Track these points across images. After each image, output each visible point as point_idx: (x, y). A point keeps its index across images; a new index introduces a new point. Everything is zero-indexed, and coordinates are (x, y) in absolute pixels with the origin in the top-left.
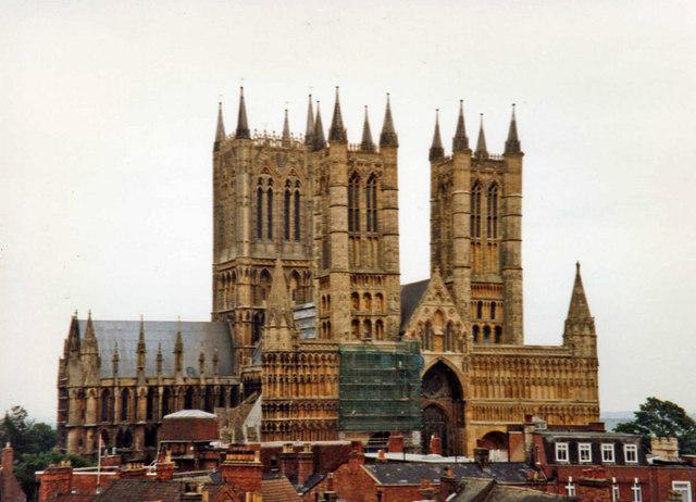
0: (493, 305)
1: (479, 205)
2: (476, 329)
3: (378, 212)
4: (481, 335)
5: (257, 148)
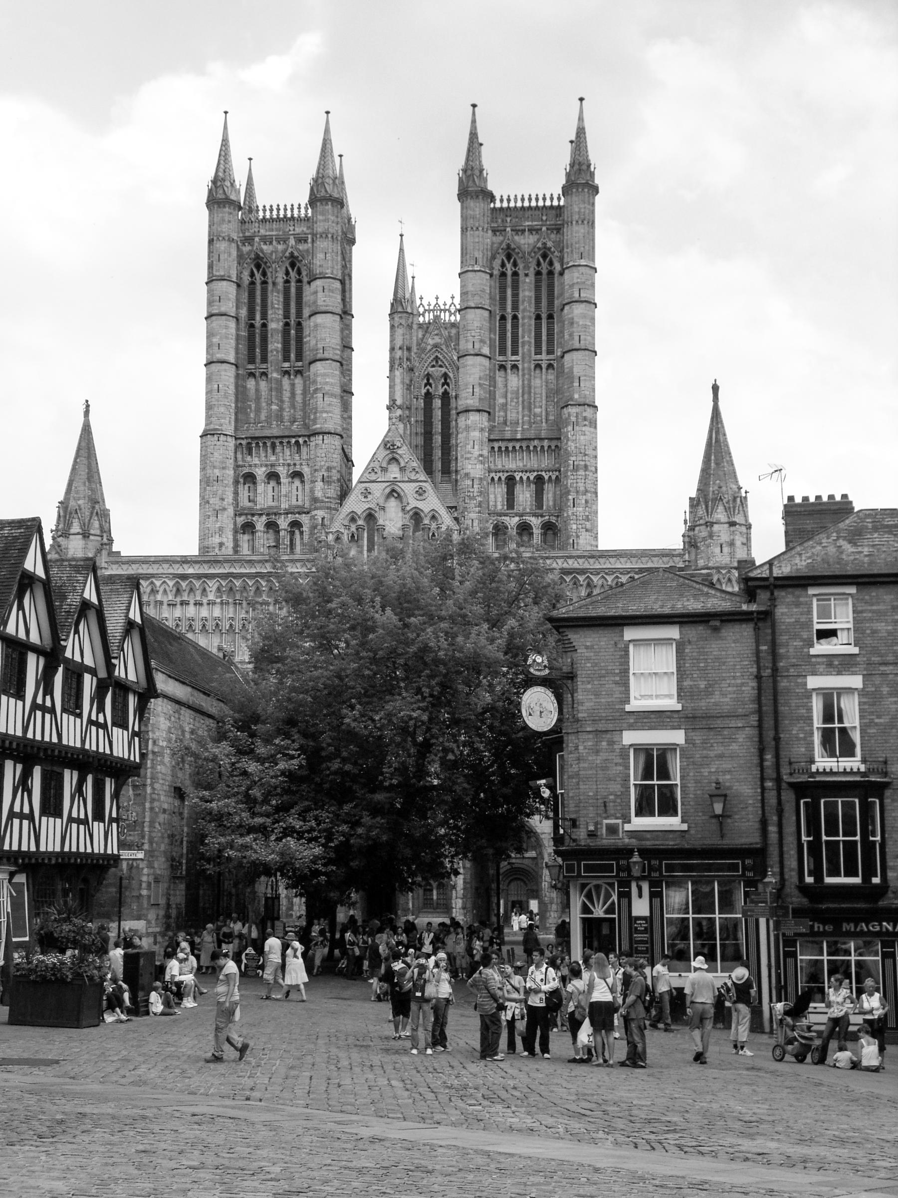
0: (539, 480)
1: (515, 295)
2: (499, 530)
3: (304, 324)
5: (420, 326)
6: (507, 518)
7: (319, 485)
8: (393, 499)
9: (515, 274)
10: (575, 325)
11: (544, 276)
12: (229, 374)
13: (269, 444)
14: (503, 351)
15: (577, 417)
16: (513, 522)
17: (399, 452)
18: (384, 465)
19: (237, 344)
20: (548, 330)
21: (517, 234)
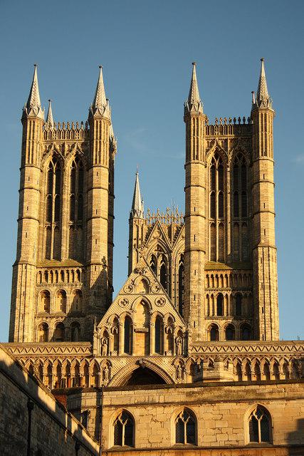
2: (214, 330)
4: (222, 335)
10: (261, 197)
11: (240, 168)
13: (59, 272)
14: (213, 215)
16: (222, 323)
19: (40, 208)
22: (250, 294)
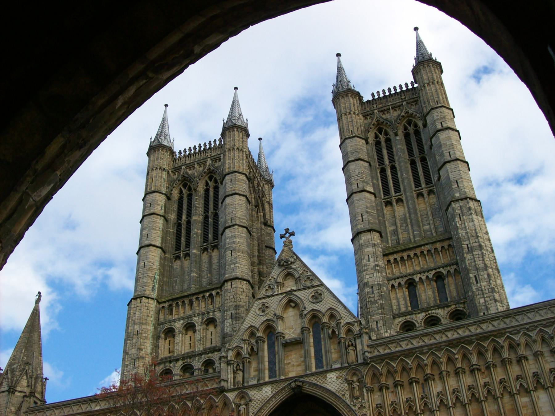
0: (439, 277)
6: (411, 316)
7: (229, 321)
8: (291, 310)
9: (388, 141)
12: (155, 255)
15: (461, 209)
17: (293, 266)
18: (280, 280)
20: (423, 168)
21: (384, 114)
22: (455, 269)
